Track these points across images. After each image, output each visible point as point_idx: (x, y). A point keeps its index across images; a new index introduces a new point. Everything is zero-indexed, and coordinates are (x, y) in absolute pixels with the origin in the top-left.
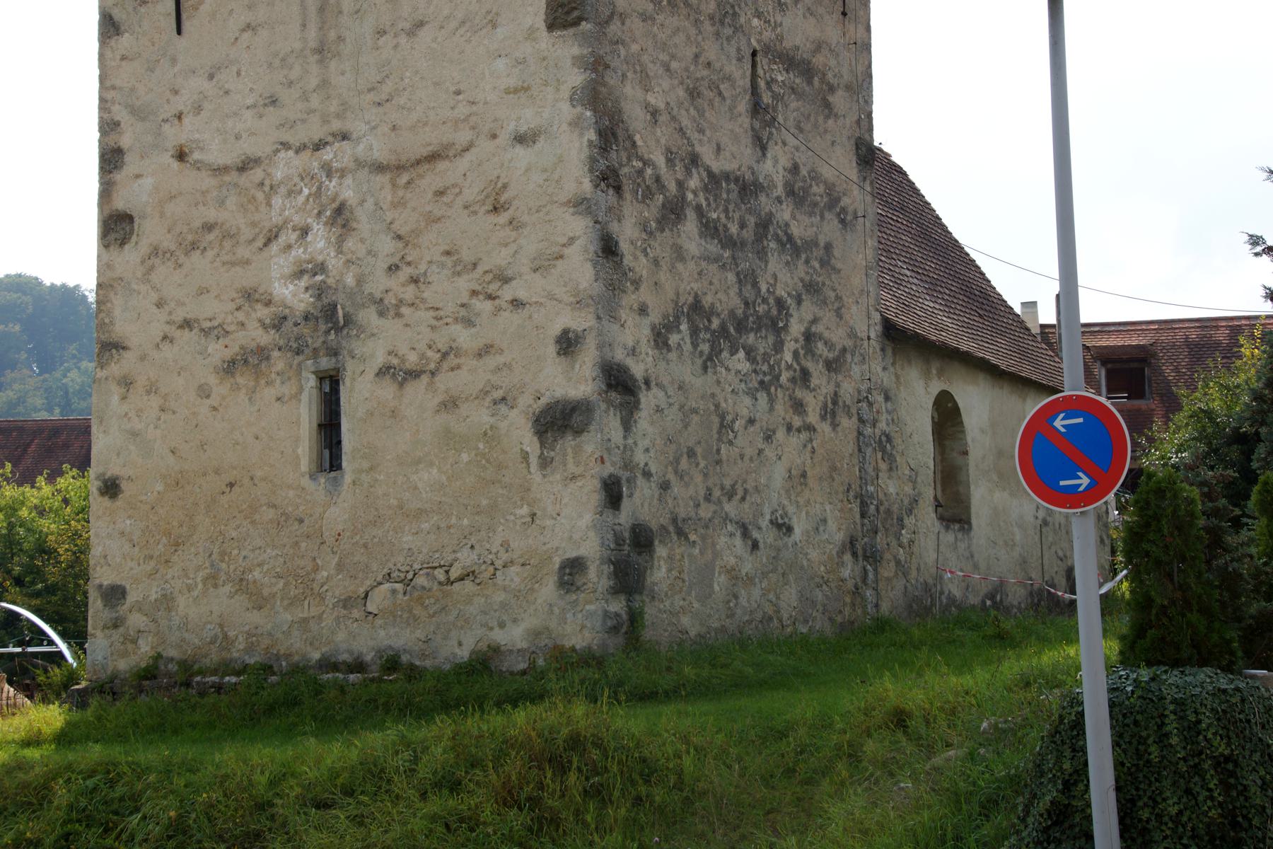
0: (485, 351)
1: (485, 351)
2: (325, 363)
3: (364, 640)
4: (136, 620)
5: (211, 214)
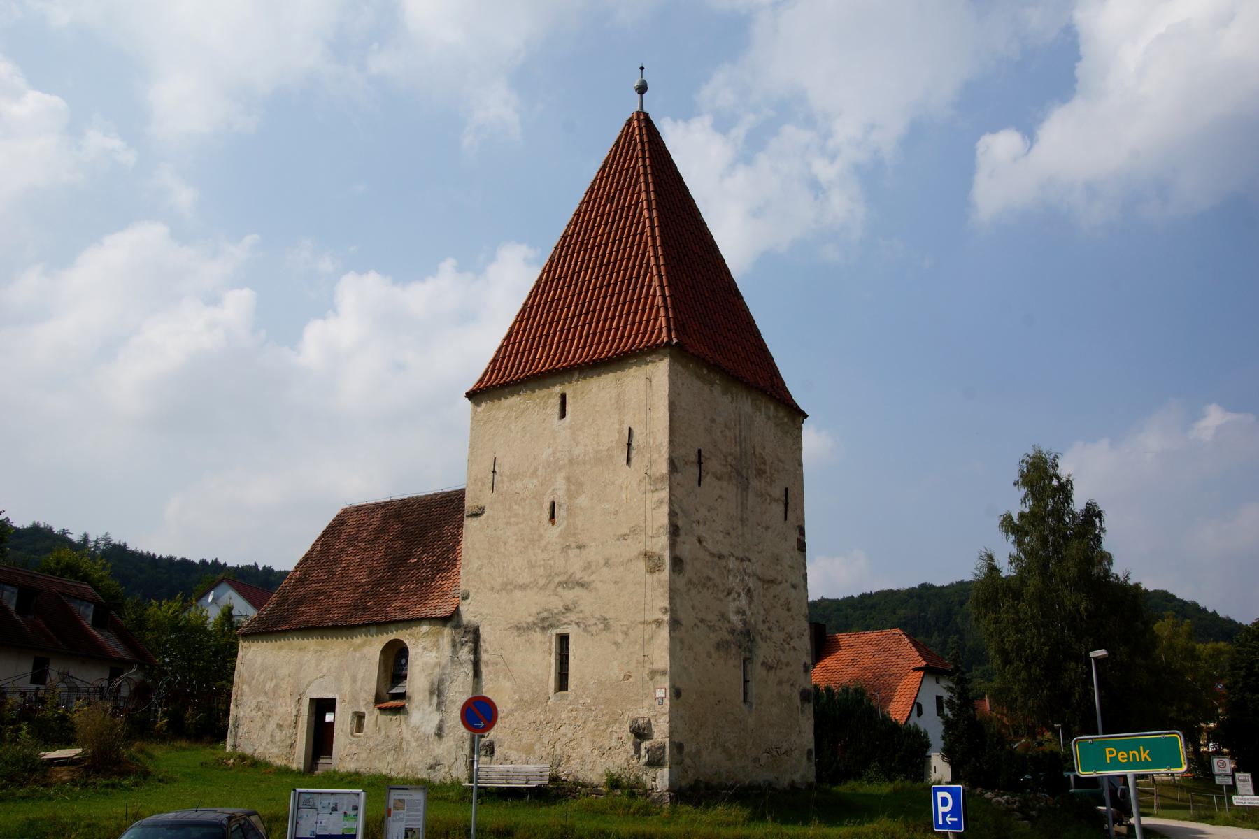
0: (788, 664)
1: (788, 664)
2: (748, 655)
3: (761, 776)
4: (688, 761)
5: (710, 573)
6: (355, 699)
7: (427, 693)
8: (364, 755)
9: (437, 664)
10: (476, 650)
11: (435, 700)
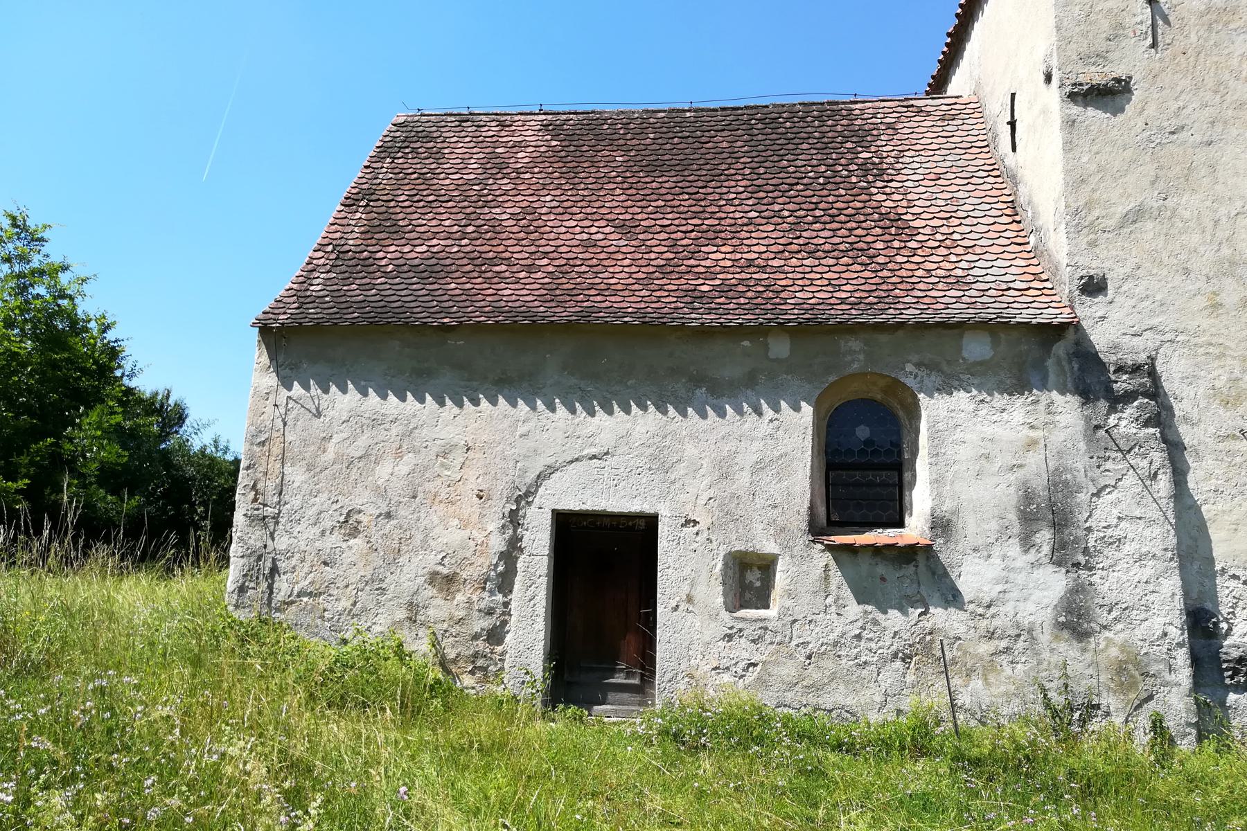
6: (729, 516)
7: (1013, 517)
8: (788, 671)
9: (1031, 444)
10: (1161, 418)
11: (1044, 537)
